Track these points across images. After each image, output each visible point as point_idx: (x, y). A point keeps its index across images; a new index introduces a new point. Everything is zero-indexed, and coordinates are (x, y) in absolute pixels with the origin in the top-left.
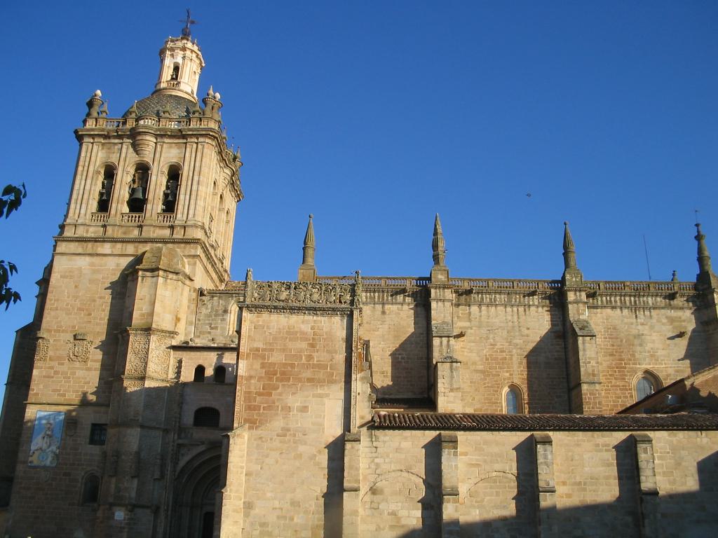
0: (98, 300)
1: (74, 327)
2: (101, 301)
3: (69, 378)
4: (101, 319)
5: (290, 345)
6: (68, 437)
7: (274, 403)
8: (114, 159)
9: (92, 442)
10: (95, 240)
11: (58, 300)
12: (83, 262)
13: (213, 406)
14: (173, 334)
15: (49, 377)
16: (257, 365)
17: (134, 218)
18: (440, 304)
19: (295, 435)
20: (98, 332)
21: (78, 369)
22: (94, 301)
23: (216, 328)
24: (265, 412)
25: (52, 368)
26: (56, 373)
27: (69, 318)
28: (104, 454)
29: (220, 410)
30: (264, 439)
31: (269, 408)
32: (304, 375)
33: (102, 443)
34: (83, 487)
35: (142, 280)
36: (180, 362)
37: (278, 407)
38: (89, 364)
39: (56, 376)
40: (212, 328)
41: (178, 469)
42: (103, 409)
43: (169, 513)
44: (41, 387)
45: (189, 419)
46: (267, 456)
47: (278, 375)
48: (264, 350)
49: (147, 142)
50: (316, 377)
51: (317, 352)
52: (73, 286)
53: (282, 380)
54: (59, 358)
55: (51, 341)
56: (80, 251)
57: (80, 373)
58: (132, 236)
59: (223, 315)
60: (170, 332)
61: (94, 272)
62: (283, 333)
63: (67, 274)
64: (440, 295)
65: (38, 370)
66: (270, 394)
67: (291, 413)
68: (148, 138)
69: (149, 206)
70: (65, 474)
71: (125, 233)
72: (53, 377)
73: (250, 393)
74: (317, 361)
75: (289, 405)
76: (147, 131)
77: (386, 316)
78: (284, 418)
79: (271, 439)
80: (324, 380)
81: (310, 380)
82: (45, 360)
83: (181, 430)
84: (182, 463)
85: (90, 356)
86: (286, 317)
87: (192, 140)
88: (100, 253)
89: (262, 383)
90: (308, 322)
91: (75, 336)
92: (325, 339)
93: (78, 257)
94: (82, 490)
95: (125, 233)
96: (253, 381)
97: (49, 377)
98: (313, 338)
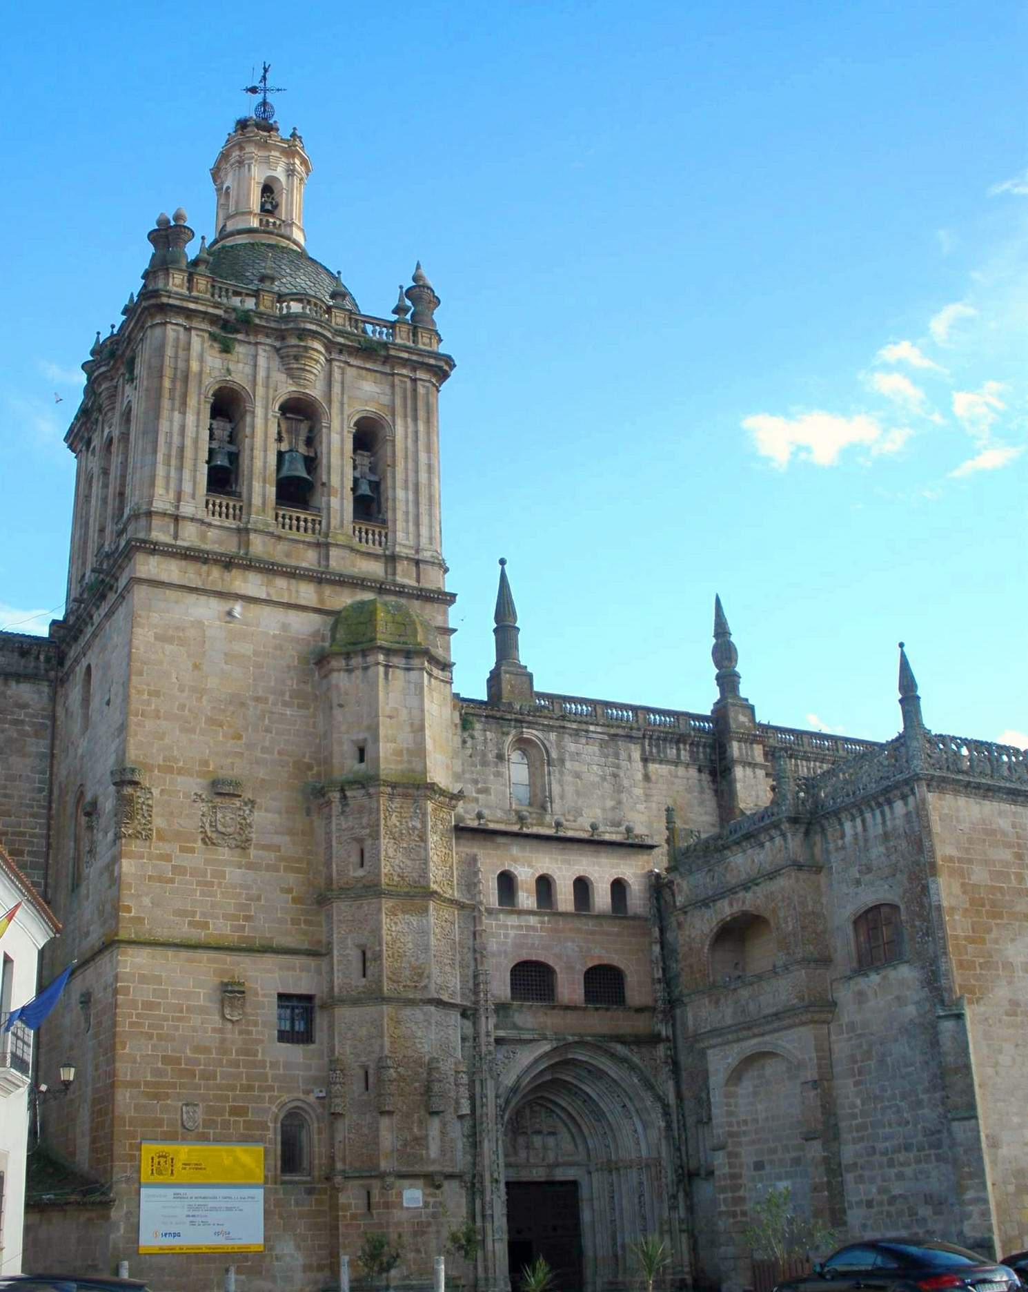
1: (206, 763)
2: (261, 706)
3: (212, 884)
4: (264, 750)
6: (229, 1025)
8: (240, 375)
9: (283, 1037)
10: (228, 563)
11: (156, 694)
12: (206, 610)
13: (542, 960)
18: (749, 771)
20: (263, 780)
22: (243, 704)
23: (485, 791)
24: (983, 972)
25: (167, 858)
29: (557, 969)
30: (990, 1021)
33: (306, 1037)
35: (386, 674)
36: (473, 860)
38: (252, 852)
39: (177, 878)
40: (479, 791)
42: (297, 961)
44: (146, 901)
45: (500, 986)
46: (1000, 1052)
47: (988, 908)
48: (960, 860)
49: (315, 355)
52: (190, 665)
54: (178, 836)
55: (156, 792)
56: (196, 582)
58: (304, 565)
59: (496, 765)
63: (171, 632)
64: (747, 755)
65: (132, 861)
68: (318, 345)
70: (235, 1111)
72: (172, 881)
76: (319, 329)
77: (651, 785)
82: (148, 838)
85: (253, 836)
87: (405, 372)
88: (242, 592)
89: (970, 921)
91: (214, 783)
93: (192, 598)
94: (279, 1147)
95: (288, 555)
97: (160, 879)
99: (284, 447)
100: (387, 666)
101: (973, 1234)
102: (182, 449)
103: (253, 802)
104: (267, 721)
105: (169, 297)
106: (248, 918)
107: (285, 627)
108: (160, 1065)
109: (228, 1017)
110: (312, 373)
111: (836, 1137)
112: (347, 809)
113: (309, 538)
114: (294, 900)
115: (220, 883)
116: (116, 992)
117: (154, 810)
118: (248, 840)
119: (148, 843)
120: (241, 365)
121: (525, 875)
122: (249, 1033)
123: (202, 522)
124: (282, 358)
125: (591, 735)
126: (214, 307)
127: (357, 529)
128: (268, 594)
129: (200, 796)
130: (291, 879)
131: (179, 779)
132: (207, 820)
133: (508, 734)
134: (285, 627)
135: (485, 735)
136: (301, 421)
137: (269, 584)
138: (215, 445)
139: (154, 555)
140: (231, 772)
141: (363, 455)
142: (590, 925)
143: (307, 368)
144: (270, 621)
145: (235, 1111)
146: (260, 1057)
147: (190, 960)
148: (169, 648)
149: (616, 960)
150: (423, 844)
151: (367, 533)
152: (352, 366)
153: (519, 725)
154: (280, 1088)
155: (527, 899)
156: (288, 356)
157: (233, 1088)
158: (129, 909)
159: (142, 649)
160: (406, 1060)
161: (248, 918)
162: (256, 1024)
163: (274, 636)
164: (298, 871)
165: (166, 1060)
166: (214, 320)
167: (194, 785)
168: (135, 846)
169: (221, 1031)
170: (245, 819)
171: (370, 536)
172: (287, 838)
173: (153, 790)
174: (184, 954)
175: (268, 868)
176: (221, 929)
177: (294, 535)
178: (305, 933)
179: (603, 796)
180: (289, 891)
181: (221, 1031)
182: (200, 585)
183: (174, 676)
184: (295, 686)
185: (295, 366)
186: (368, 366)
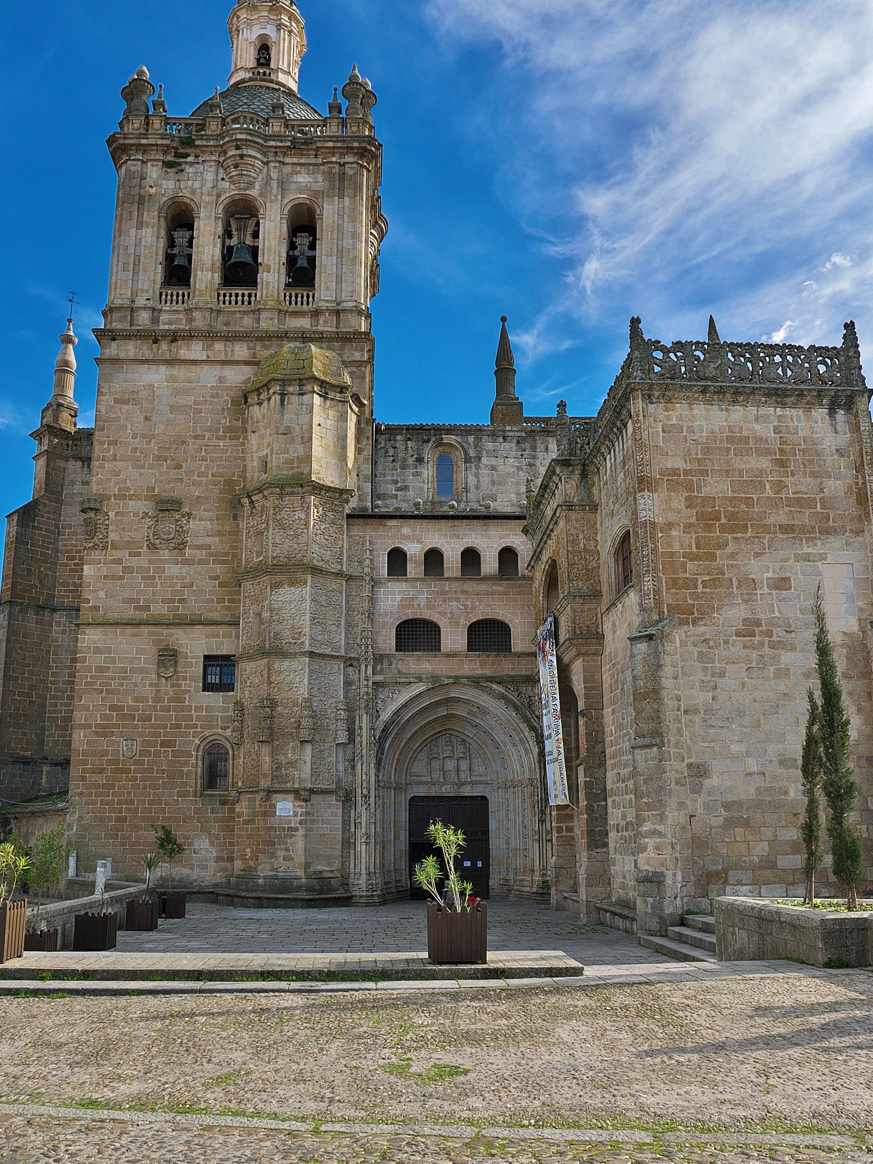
0: (191, 441)
5: (738, 463)
6: (164, 680)
7: (723, 573)
9: (207, 687)
14: (342, 494)
15: (113, 578)
16: (678, 501)
17: (240, 298)
19: (770, 634)
21: (166, 561)
23: (405, 488)
25: (119, 561)
26: (128, 570)
27: (141, 474)
28: (239, 706)
31: (714, 583)
32: (771, 520)
33: (228, 687)
34: (200, 763)
37: (731, 580)
38: (188, 551)
40: (398, 490)
41: (380, 725)
42: (221, 630)
43: (372, 800)
44: (102, 594)
49: (249, 160)
50: (796, 522)
51: (793, 475)
52: (142, 418)
53: (732, 531)
55: (112, 514)
56: (148, 355)
57: (172, 570)
60: (342, 492)
61: (177, 392)
62: (722, 441)
66: (713, 557)
67: (758, 592)
69: (263, 276)
71: (227, 324)
72: (122, 578)
73: (672, 555)
74: (793, 493)
75: (751, 576)
78: (746, 601)
79: (726, 642)
80: (813, 528)
81: (786, 529)
82: (105, 548)
83: (379, 659)
84: (385, 715)
85: (188, 539)
86: (722, 410)
90: (765, 419)
92: (804, 451)
96: (674, 533)
97: (113, 578)
98: (781, 451)
99: (234, 242)
100: (283, 395)
101: (647, 867)
102: (137, 258)
103: (189, 515)
104: (203, 454)
105: (125, 138)
106: (181, 601)
107: (221, 379)
108: (107, 712)
109: (162, 674)
110: (250, 176)
111: (602, 764)
112: (254, 511)
113: (244, 308)
114: (221, 585)
115: (160, 577)
116: (74, 660)
117: (110, 528)
118: (182, 543)
119: (104, 552)
120: (190, 183)
121: (414, 550)
122: (179, 686)
123: (154, 310)
124: (225, 170)
125: (508, 434)
126: (162, 138)
127: (288, 294)
128: (208, 356)
129: (147, 514)
130: (219, 569)
131: (130, 503)
132: (151, 531)
133: (428, 441)
134: (221, 379)
135: (407, 444)
136: (249, 218)
137: (209, 348)
138: (176, 251)
139: (114, 339)
140: (172, 494)
141: (301, 237)
142: (483, 587)
143: (244, 172)
144: (209, 376)
145: (164, 744)
146: (187, 703)
147: (135, 635)
148: (125, 407)
149: (501, 613)
150: (305, 531)
151: (296, 297)
152: (287, 164)
153: (438, 432)
154: (202, 727)
155: (415, 569)
156: (229, 167)
157: (165, 727)
158: (88, 601)
159: (104, 411)
160: (285, 701)
161: (181, 601)
162: (185, 678)
163: (212, 388)
164: (225, 562)
165: (112, 708)
166: (166, 150)
167: (144, 506)
168: (95, 555)
169: (157, 685)
170: (182, 527)
171: (299, 299)
172: (217, 539)
173: (110, 513)
174: (130, 630)
175: (200, 562)
176: (159, 609)
177: (233, 308)
178: (228, 609)
179: (518, 483)
180: (216, 578)
181: (157, 685)
182: (151, 357)
183: (129, 427)
184: (228, 424)
185: (234, 173)
186: (301, 161)
